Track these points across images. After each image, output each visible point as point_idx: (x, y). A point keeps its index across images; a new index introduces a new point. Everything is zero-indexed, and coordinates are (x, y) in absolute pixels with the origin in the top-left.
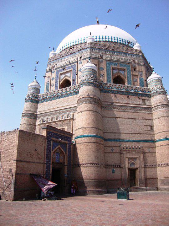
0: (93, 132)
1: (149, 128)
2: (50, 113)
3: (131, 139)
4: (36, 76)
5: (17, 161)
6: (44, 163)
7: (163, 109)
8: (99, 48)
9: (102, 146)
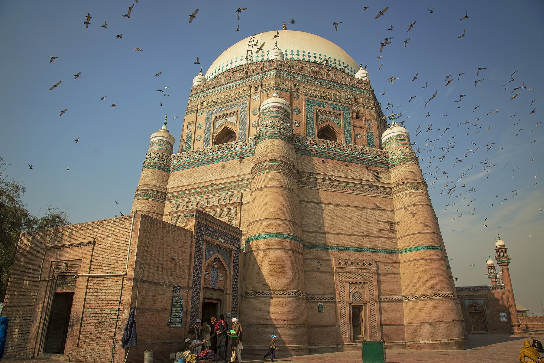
1: (387, 227)
2: (193, 191)
4: (166, 120)
5: (136, 280)
6: (189, 288)
8: (288, 73)
9: (301, 256)
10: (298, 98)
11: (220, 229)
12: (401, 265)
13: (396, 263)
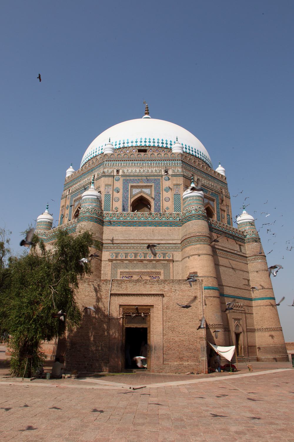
2: (129, 245)
12: (253, 308)
13: (250, 306)
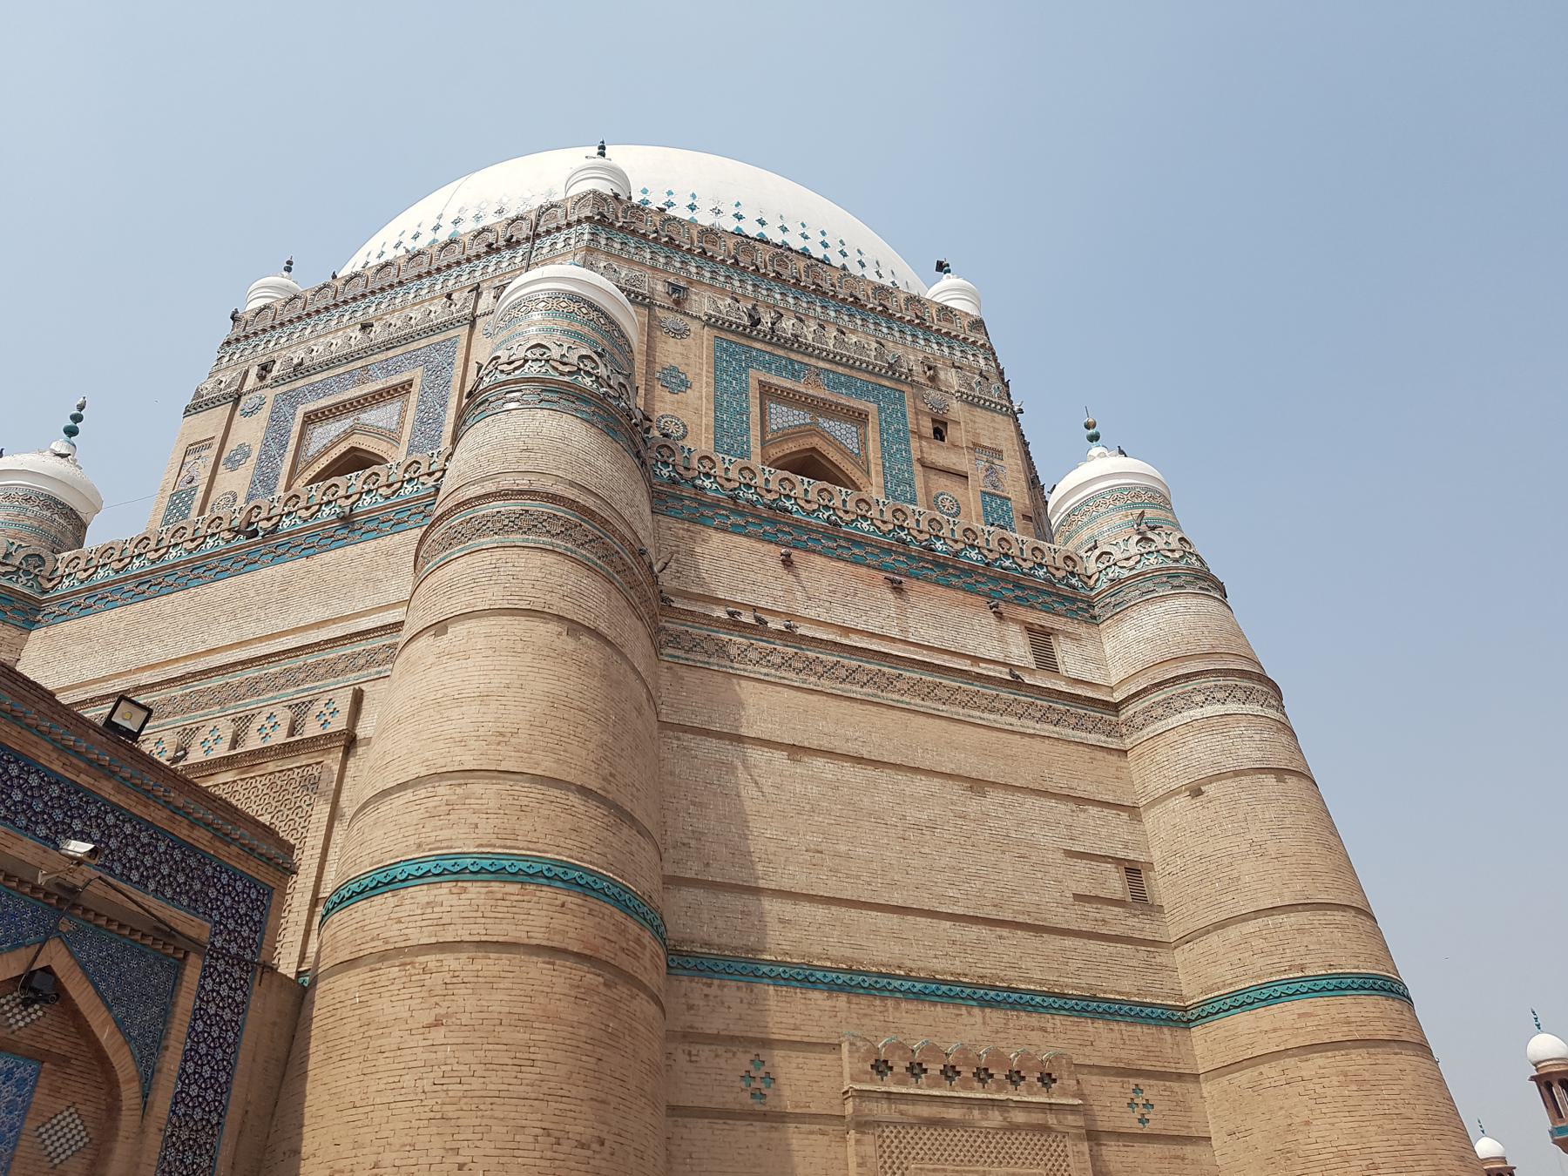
0: (552, 830)
1: (1115, 883)
3: (944, 965)
7: (1219, 709)
10: (680, 333)
11: (107, 789)
13: (1180, 1077)
